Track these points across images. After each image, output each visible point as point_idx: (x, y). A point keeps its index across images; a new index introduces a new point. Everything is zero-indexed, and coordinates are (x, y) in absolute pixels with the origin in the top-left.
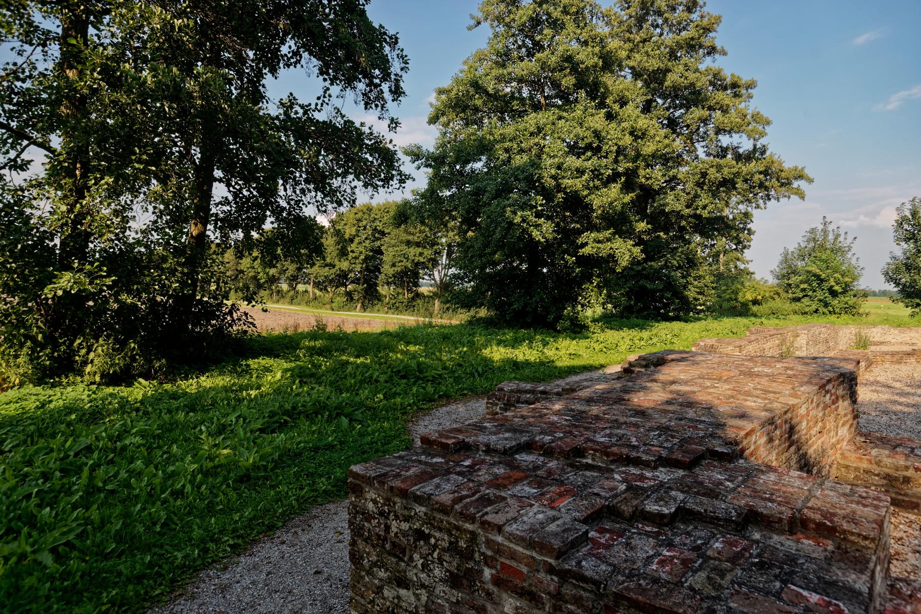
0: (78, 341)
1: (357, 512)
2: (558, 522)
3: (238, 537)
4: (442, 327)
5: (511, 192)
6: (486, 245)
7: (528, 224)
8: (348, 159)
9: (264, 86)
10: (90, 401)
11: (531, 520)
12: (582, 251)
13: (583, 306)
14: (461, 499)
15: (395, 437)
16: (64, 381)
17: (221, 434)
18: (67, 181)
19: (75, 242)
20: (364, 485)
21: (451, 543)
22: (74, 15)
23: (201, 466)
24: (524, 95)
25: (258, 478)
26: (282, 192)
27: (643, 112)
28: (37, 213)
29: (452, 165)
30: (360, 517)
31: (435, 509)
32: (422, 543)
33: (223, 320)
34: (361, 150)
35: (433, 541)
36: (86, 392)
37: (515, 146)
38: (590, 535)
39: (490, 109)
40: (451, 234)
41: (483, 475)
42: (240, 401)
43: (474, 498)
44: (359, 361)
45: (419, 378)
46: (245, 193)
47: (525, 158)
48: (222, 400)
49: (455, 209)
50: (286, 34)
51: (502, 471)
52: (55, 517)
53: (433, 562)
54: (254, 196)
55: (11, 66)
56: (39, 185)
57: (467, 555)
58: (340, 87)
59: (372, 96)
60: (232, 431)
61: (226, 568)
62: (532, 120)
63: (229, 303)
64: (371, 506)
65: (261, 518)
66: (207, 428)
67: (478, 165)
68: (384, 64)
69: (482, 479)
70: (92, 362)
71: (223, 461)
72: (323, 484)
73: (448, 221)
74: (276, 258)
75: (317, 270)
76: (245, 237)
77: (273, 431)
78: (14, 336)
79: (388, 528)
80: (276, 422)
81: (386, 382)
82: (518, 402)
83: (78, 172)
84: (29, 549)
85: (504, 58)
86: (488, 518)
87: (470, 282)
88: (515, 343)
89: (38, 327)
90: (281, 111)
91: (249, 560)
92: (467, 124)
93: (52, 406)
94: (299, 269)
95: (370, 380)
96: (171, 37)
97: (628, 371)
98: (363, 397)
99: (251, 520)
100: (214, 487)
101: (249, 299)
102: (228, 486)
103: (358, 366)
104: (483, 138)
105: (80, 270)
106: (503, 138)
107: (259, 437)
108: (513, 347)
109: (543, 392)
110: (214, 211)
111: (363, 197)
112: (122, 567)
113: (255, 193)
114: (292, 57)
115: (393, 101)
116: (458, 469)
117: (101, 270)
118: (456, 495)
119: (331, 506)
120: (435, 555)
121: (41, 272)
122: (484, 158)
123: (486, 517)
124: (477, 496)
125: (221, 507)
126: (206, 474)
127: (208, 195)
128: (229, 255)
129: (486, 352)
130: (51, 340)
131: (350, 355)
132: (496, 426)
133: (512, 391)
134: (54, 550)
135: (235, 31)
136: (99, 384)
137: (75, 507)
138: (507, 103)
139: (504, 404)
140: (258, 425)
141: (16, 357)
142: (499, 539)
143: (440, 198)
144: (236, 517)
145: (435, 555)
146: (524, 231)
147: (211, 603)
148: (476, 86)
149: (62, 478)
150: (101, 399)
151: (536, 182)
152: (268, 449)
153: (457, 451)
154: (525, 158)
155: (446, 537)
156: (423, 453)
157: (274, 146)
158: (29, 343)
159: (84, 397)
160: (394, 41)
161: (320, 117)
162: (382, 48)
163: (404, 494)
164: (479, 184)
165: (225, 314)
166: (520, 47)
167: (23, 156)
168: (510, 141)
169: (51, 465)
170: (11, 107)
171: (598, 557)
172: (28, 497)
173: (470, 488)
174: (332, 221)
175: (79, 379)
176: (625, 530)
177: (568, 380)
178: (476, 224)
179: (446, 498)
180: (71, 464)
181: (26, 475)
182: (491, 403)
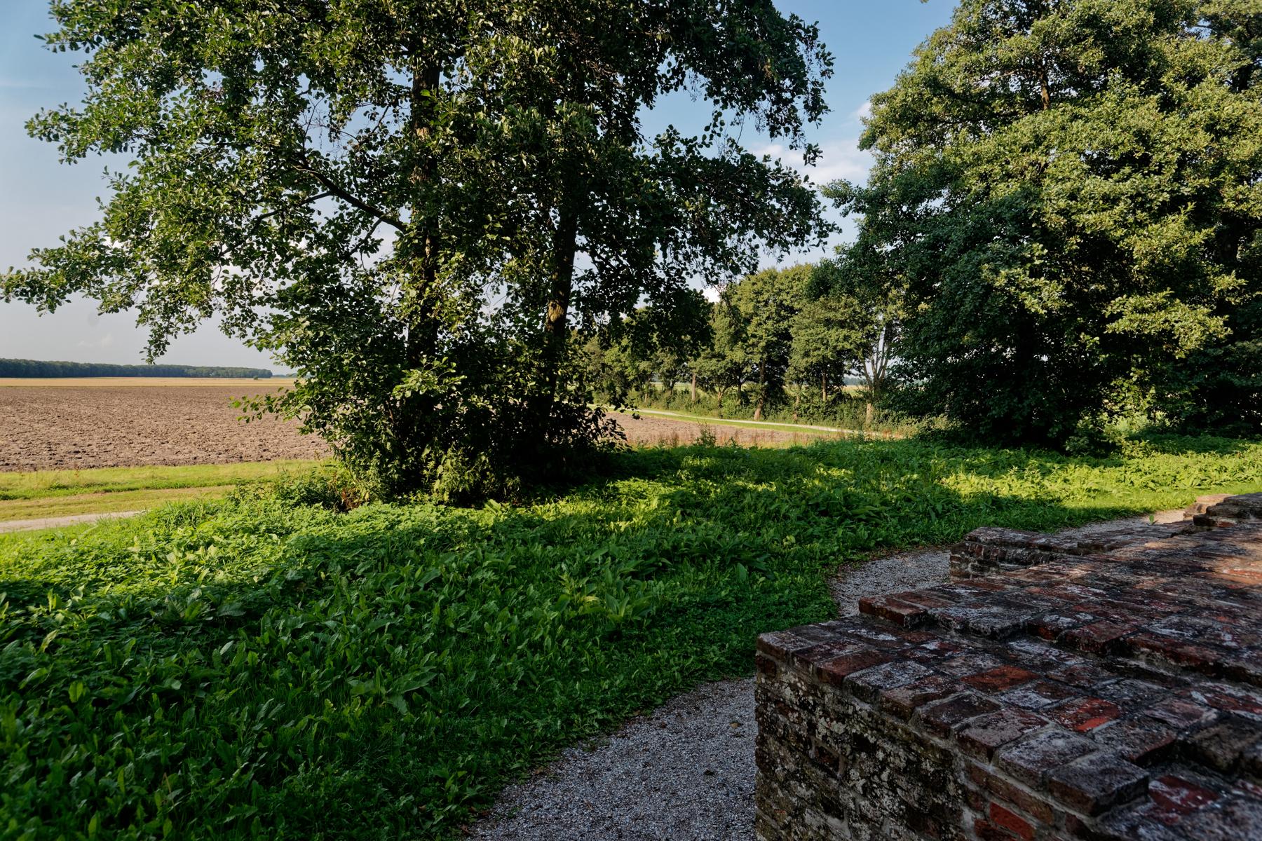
1: (769, 699)
2: (1093, 757)
3: (608, 711)
4: (878, 442)
5: (990, 240)
6: (949, 322)
7: (1018, 287)
8: (746, 208)
9: (637, 121)
11: (1043, 747)
12: (1111, 327)
13: (1111, 413)
14: (926, 699)
15: (813, 598)
16: (413, 498)
17: (585, 576)
18: (415, 261)
20: (779, 663)
21: (908, 762)
22: (428, 62)
23: (563, 614)
24: (1012, 90)
25: (631, 637)
26: (659, 259)
27: (1232, 90)
28: (387, 300)
29: (895, 207)
30: (771, 707)
31: (885, 709)
32: (864, 755)
33: (585, 429)
34: (764, 195)
35: (881, 755)
37: (997, 169)
38: (1150, 787)
39: (954, 117)
40: (891, 308)
41: (959, 666)
42: (607, 534)
43: (946, 701)
44: (760, 488)
45: (846, 516)
46: (614, 263)
47: (1014, 186)
48: (585, 532)
49: (900, 270)
50: (664, 49)
51: (991, 664)
52: (408, 658)
53: (880, 786)
54: (625, 266)
56: (389, 268)
57: (935, 784)
58: (736, 110)
59: (781, 116)
60: (598, 572)
61: (593, 749)
62: (1025, 126)
63: (593, 407)
64: (788, 693)
65: (636, 690)
66: (569, 566)
67: (936, 204)
68: (796, 70)
69: (957, 672)
71: (588, 611)
72: (714, 654)
73: (889, 289)
74: (653, 348)
75: (702, 364)
76: (612, 320)
77: (649, 577)
78: (364, 444)
79: (812, 727)
80: (652, 565)
81: (799, 519)
82: (1002, 559)
83: (427, 250)
85: (980, 34)
86: (973, 733)
87: (922, 378)
88: (995, 469)
89: (387, 434)
90: (659, 151)
91: (622, 743)
92: (919, 145)
93: (401, 527)
94: (679, 362)
95: (775, 516)
96: (529, 72)
97: (1203, 522)
98: (767, 538)
99: (623, 691)
100: (577, 642)
101: (617, 402)
102: (595, 643)
103: (759, 495)
104: (945, 161)
105: (429, 367)
106: (978, 159)
107: (631, 583)
108: (991, 476)
109: (1044, 547)
110: (575, 288)
111: (768, 260)
112: (476, 728)
113: (625, 262)
114: (672, 78)
115: (810, 120)
116: (918, 654)
118: (918, 692)
119: (725, 685)
120: (884, 776)
121: (390, 369)
122: (945, 192)
123: (967, 732)
124: (951, 697)
125: (586, 669)
126: (569, 625)
127: (567, 268)
128: (592, 345)
129: (949, 482)
130: (399, 451)
131: (748, 479)
132: (976, 595)
133: (993, 542)
135: (605, 54)
138: (983, 104)
139: (980, 562)
140: (630, 568)
141: (366, 468)
142: (990, 768)
143: (877, 256)
144: (605, 685)
145: (884, 776)
146: (1011, 298)
147: (577, 791)
148: (934, 84)
149: (413, 612)
150: (451, 522)
151: (1031, 222)
152: (643, 601)
153: (916, 627)
154: (1014, 186)
155: (901, 753)
156: (864, 625)
157: (651, 198)
158: (378, 453)
159: (433, 519)
160: (813, 33)
161: (709, 153)
162: (794, 47)
163: (837, 681)
164: (938, 232)
165: (588, 421)
166: (1006, 15)
167: (373, 236)
168: (988, 162)
169: (402, 597)
170: (363, 180)
171: (1169, 825)
172: (381, 630)
173: (938, 685)
174: (725, 296)
175: (427, 497)
176: (1219, 789)
177: (1087, 530)
178: (932, 291)
179: (903, 695)
180: (421, 597)
181: (378, 606)
182: (958, 559)
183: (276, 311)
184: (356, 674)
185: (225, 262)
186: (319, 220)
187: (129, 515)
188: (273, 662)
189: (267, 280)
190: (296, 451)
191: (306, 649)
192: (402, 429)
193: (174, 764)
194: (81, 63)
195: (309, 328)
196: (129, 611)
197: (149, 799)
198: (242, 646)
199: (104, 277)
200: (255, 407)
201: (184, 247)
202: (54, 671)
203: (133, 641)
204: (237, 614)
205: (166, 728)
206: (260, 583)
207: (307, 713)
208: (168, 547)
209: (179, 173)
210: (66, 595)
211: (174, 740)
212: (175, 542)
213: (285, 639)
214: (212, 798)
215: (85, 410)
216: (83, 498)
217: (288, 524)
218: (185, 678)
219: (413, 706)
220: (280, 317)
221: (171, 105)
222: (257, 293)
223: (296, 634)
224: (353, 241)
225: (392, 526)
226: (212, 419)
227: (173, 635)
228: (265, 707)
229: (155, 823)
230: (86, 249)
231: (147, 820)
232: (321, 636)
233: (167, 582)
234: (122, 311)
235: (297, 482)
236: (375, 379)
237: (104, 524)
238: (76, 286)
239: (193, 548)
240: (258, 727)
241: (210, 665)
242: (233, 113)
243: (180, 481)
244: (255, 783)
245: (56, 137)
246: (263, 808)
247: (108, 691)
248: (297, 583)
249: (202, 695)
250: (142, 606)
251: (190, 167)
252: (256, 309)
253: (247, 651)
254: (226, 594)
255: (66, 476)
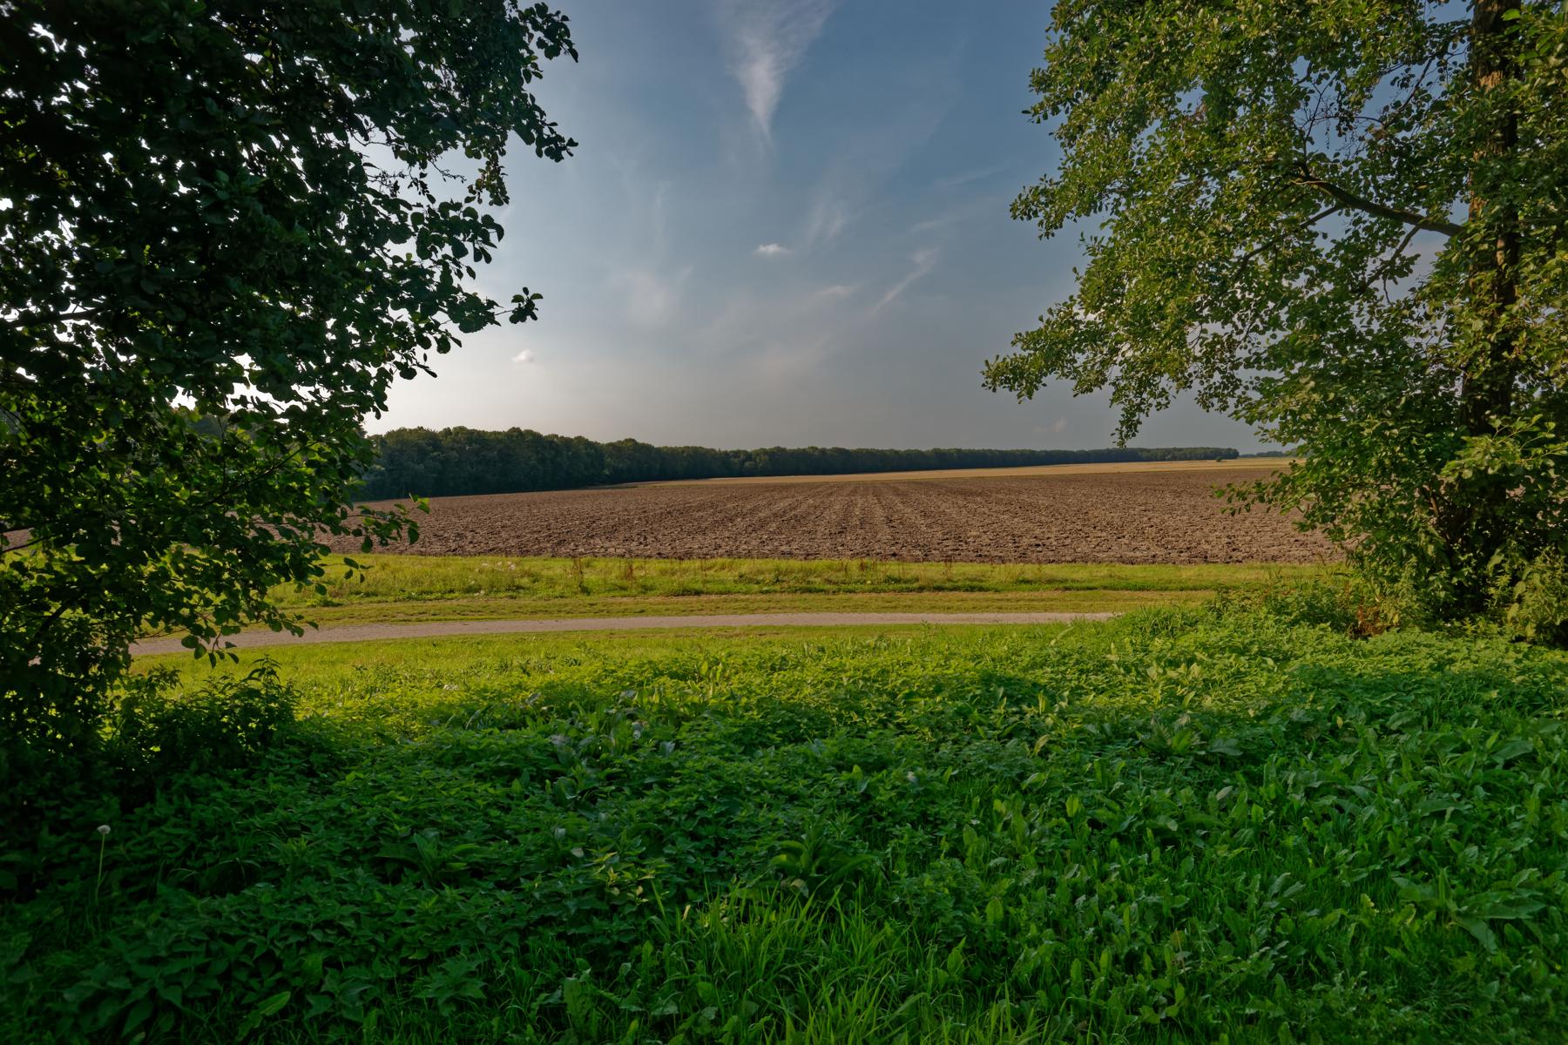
0: (1496, 559)
10: (1522, 673)
19: (1493, 384)
36: (1511, 653)
55: (1391, 111)
70: (1520, 600)
84: (1453, 907)
117: (1545, 429)
134: (1495, 925)
136: (1534, 642)
137: (1521, 862)
150: (1543, 671)
183: (1264, 373)
184: (1403, 869)
185: (1205, 320)
186: (1323, 246)
187: (1102, 616)
188: (1283, 824)
189: (1253, 335)
190: (1274, 551)
191: (1326, 817)
192: (1453, 523)
193: (1175, 920)
194: (1056, 129)
195: (1314, 390)
196: (1114, 727)
197: (1156, 951)
198: (1245, 795)
199: (1077, 355)
200: (1242, 496)
201: (1160, 308)
202: (1050, 779)
203: (1121, 764)
204: (1231, 753)
205: (1165, 874)
206: (1258, 718)
207: (1337, 905)
208: (1147, 660)
209: (1155, 222)
210: (1053, 699)
211: (1176, 893)
212: (1155, 654)
213: (1298, 799)
214: (1225, 976)
215: (1044, 501)
216: (1045, 595)
217: (1287, 647)
218: (1181, 819)
219: (1503, 941)
220: (1269, 380)
221: (1146, 145)
222: (1240, 354)
223: (1310, 793)
224: (1372, 265)
225: (1439, 667)
226: (1171, 510)
227: (1160, 763)
228: (1279, 881)
229: (1164, 982)
230: (1062, 326)
231: (1155, 975)
232: (1348, 805)
233: (1149, 700)
234: (1096, 389)
235: (1296, 593)
236: (1412, 454)
237: (1079, 626)
238: (1051, 368)
239: (1174, 664)
240: (1274, 904)
241: (1204, 809)
242: (1217, 133)
243: (1140, 582)
244: (1279, 978)
245: (1035, 213)
246: (1292, 1014)
247: (1102, 814)
248: (1305, 726)
249: (1201, 844)
250: (1126, 724)
251: (1165, 213)
252: (1243, 374)
253: (1250, 803)
254: (1216, 726)
255: (1030, 570)
